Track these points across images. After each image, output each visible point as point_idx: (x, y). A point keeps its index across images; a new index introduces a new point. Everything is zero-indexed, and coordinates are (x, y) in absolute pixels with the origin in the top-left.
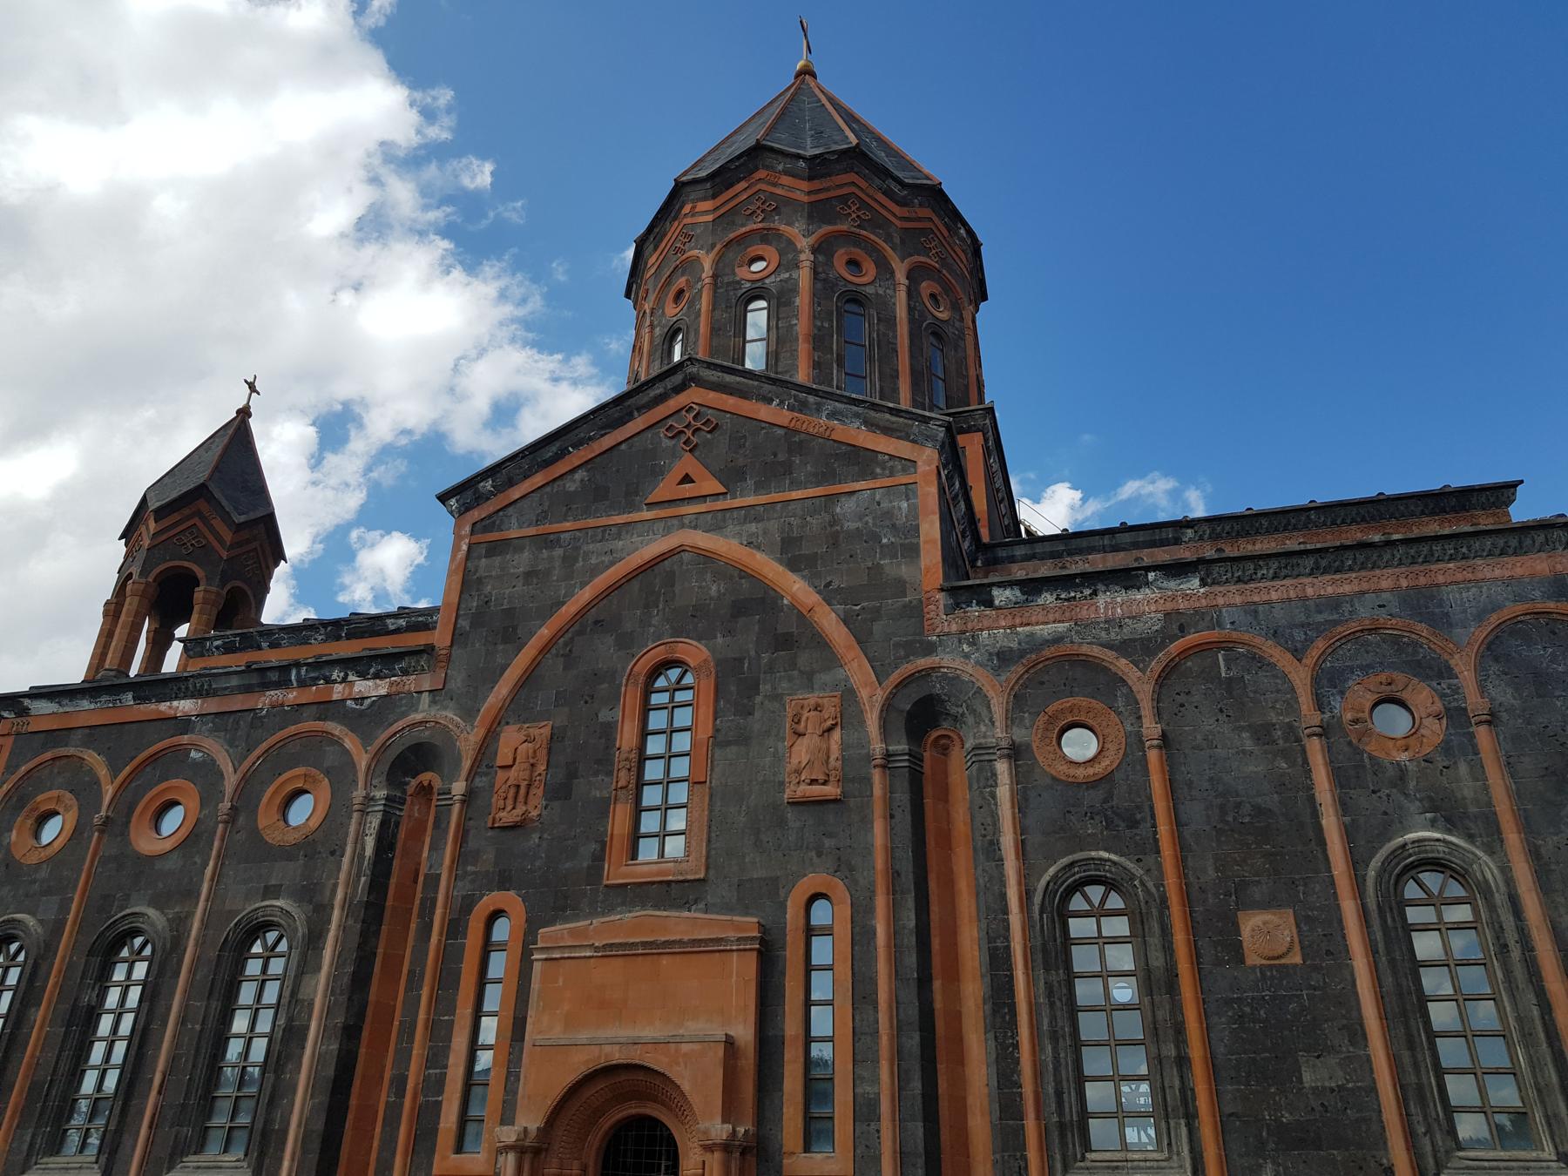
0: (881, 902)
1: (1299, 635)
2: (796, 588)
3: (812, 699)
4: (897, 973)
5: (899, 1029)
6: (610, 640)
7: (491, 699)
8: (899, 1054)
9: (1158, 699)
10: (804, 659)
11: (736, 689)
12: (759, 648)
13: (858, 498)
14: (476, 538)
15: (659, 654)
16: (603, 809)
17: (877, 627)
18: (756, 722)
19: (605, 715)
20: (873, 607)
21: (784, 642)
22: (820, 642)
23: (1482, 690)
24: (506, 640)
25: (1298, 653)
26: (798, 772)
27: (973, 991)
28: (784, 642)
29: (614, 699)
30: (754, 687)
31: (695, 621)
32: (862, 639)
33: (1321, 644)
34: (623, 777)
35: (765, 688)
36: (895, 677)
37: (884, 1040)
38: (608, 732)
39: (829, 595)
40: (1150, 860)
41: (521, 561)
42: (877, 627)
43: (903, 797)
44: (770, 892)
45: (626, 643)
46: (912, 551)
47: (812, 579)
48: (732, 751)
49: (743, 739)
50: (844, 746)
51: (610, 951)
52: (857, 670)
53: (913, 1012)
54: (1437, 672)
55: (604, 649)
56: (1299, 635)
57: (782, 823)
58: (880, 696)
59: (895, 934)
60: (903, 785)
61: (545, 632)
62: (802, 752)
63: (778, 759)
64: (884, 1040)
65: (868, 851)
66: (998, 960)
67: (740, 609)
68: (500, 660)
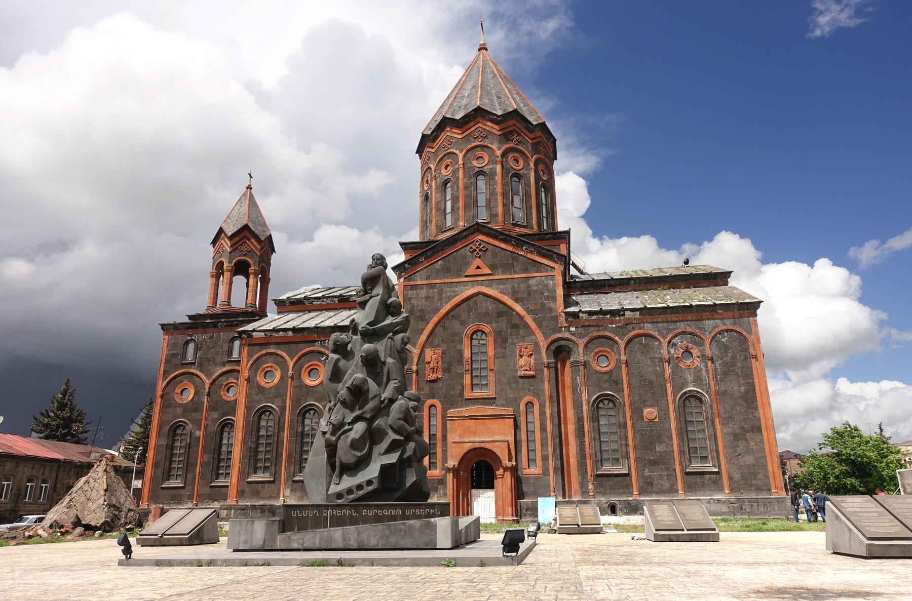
0: (547, 404)
1: (665, 332)
2: (518, 308)
3: (525, 344)
4: (553, 424)
5: (554, 437)
6: (458, 322)
7: (420, 340)
8: (554, 444)
9: (625, 349)
10: (521, 332)
11: (501, 340)
12: (509, 328)
13: (537, 277)
14: (407, 283)
15: (474, 328)
16: (462, 376)
17: (544, 323)
18: (508, 351)
19: (459, 347)
20: (544, 315)
21: (515, 326)
22: (527, 326)
23: (711, 349)
24: (422, 320)
25: (664, 337)
26: (522, 367)
27: (571, 428)
28: (515, 326)
29: (461, 342)
30: (505, 340)
31: (485, 317)
32: (540, 326)
33: (671, 335)
34: (467, 367)
35: (510, 341)
36: (550, 339)
37: (550, 441)
38: (461, 352)
39: (529, 311)
40: (621, 394)
41: (423, 292)
42: (544, 323)
43: (553, 375)
44: (515, 402)
45: (463, 324)
46: (554, 298)
47: (523, 306)
48: (501, 360)
49: (504, 356)
50: (535, 360)
51: (471, 418)
52: (540, 337)
53: (557, 433)
54: (700, 343)
55: (456, 325)
56: (665, 332)
57: (517, 382)
58: (546, 346)
59: (552, 413)
60: (553, 370)
61: (435, 319)
62: (522, 362)
63: (515, 363)
64: (550, 441)
65: (543, 390)
66: (580, 420)
67: (500, 314)
68: (421, 327)
